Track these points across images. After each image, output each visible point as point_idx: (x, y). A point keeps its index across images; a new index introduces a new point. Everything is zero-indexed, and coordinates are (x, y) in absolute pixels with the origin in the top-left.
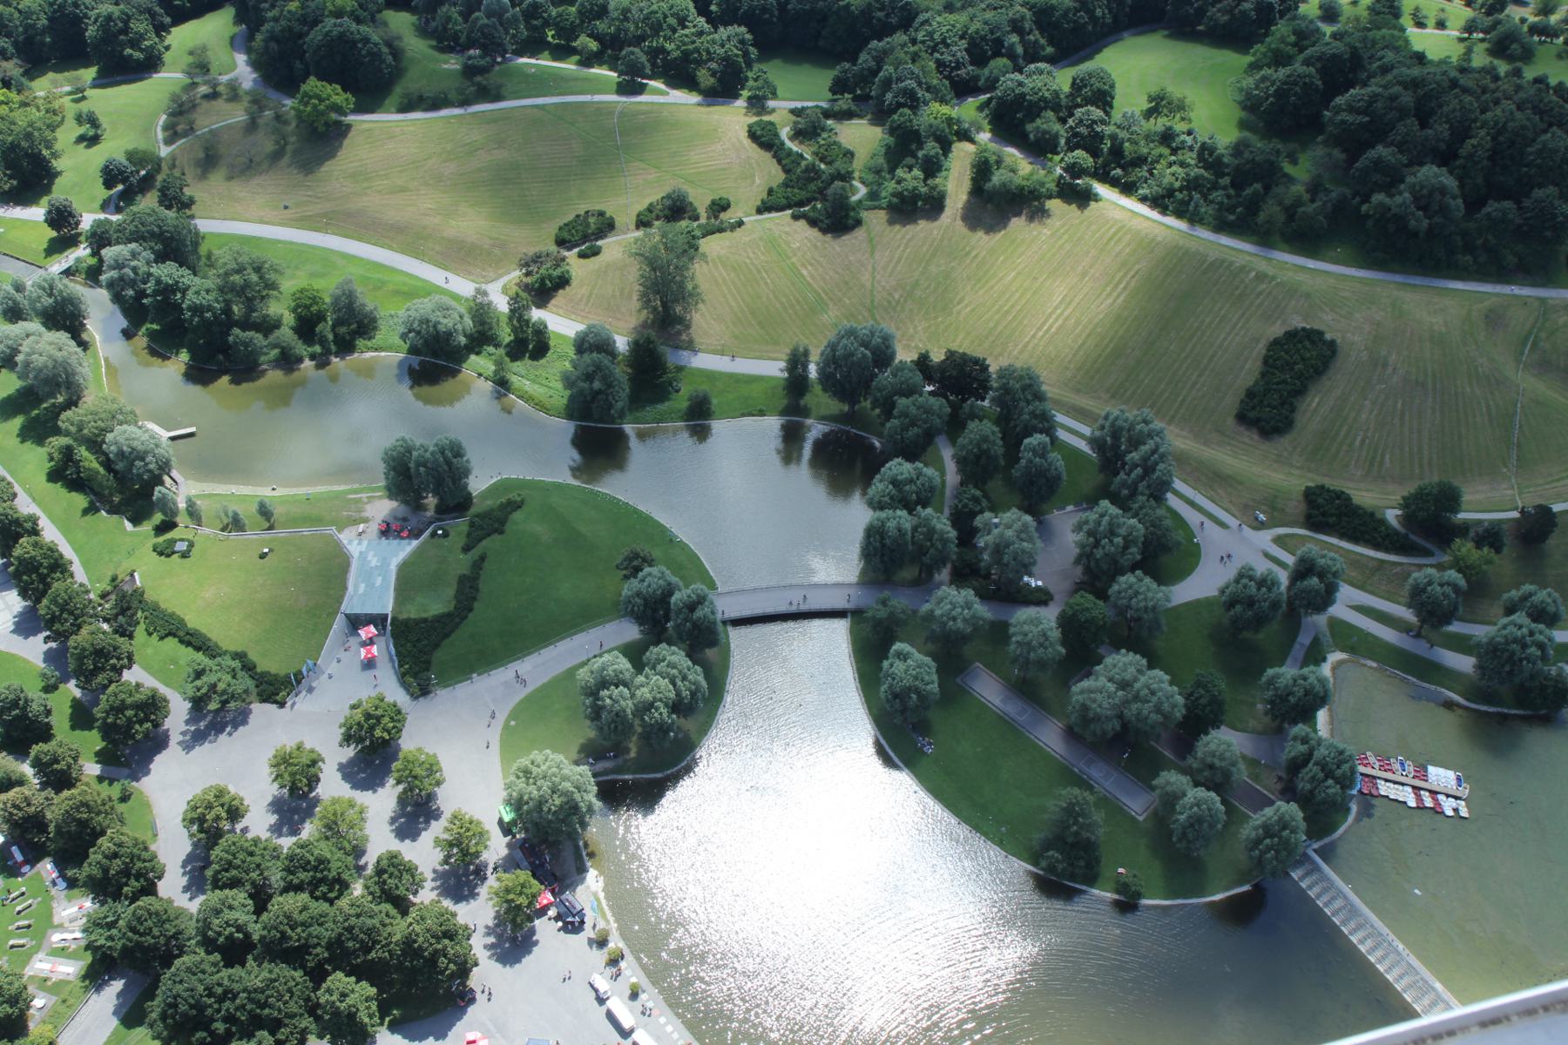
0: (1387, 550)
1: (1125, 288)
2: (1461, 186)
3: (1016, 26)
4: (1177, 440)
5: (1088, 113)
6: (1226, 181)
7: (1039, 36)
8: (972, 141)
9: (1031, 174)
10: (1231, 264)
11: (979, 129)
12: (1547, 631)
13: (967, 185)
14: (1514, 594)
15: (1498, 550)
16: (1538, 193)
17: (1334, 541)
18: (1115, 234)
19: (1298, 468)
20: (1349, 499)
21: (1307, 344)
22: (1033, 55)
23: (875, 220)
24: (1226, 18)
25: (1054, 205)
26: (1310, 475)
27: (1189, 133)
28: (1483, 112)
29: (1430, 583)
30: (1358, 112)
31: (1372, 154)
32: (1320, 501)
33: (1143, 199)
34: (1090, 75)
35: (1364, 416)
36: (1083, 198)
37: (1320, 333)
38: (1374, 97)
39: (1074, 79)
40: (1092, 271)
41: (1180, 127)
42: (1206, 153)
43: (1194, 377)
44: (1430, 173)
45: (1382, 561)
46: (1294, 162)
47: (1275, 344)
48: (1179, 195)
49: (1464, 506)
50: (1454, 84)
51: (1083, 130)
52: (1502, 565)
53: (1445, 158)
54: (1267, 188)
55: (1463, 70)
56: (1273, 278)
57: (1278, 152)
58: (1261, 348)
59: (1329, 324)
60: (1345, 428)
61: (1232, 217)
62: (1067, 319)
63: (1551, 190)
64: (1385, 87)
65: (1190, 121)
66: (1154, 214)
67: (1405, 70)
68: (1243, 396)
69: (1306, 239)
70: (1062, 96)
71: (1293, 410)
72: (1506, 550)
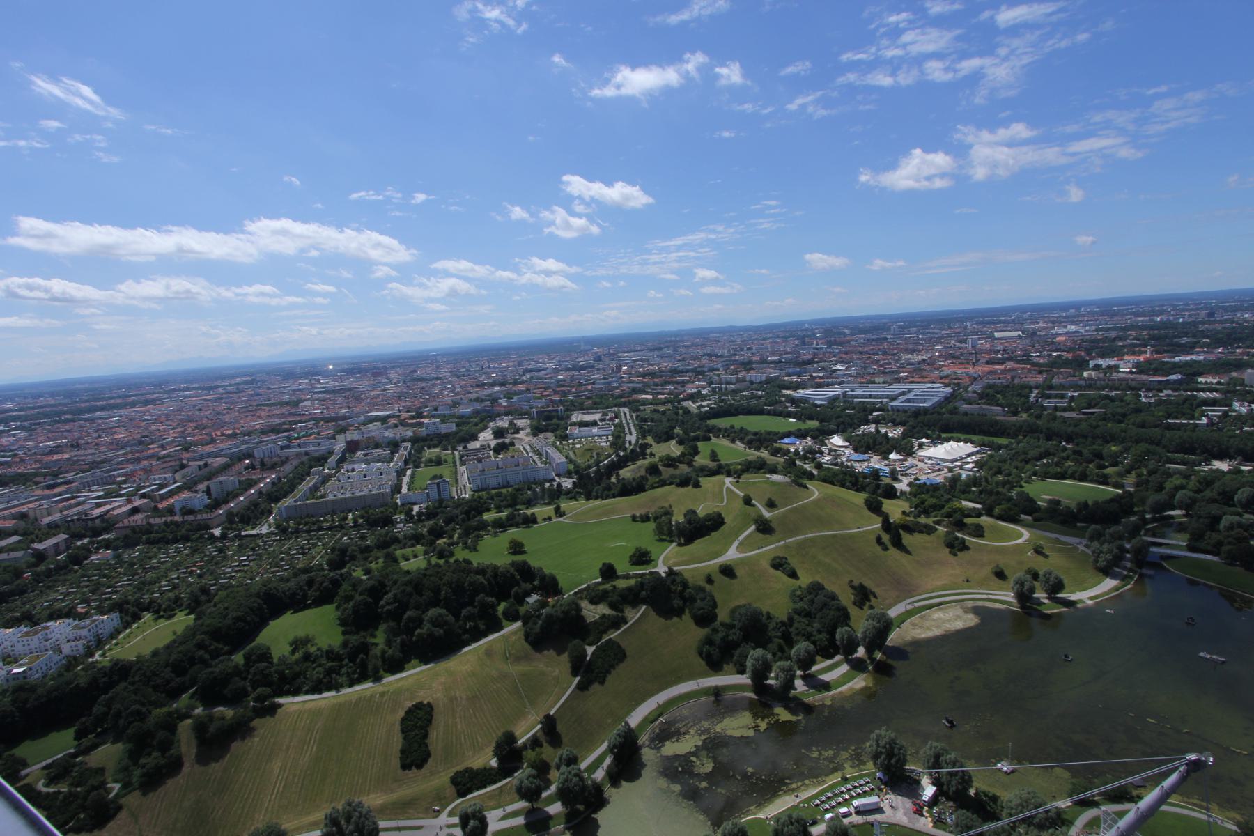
0: (500, 781)
1: (315, 741)
2: (448, 610)
3: (200, 646)
4: (373, 800)
5: (257, 668)
6: (346, 661)
7: (216, 644)
8: (189, 716)
9: (234, 715)
10: (365, 697)
11: (194, 708)
12: (576, 767)
13: (194, 742)
14: (557, 760)
15: (541, 746)
16: (478, 599)
17: (475, 794)
18: (298, 716)
19: (444, 771)
20: (471, 768)
21: (418, 711)
22: (216, 654)
23: (133, 799)
24: (318, 593)
25: (256, 722)
26: (449, 771)
27: (318, 649)
28: (441, 580)
29: (522, 782)
30: (391, 603)
31: (405, 616)
32: (459, 780)
33: (307, 693)
34: (252, 649)
35: (459, 727)
36: (273, 709)
37: (421, 703)
38: (395, 595)
39: (244, 655)
40: (292, 744)
41: (313, 649)
42: (331, 655)
43: (371, 762)
44: (433, 612)
45: (501, 787)
46: (374, 636)
47: (403, 719)
48: (325, 680)
49: (518, 737)
50: (425, 575)
51: (258, 677)
52: (549, 753)
53: (435, 603)
54: (367, 654)
55: (426, 569)
56: (388, 691)
57: (364, 636)
58: (398, 727)
59: (424, 697)
60: (454, 738)
61: (356, 676)
62: (287, 777)
63: (482, 595)
64: (398, 589)
65: (317, 644)
66: (316, 696)
67: (403, 579)
68: (399, 755)
69: (395, 666)
70: (240, 667)
71: (427, 746)
72: (545, 744)
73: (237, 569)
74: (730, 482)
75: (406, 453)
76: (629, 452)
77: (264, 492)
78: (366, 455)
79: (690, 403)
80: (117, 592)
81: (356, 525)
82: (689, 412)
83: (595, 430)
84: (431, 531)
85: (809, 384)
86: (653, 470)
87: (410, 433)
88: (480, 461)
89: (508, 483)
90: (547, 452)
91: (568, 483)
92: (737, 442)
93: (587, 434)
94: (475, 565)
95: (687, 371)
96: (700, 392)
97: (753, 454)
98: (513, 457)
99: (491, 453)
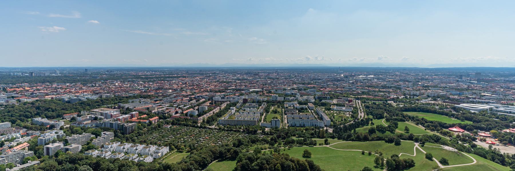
73: (204, 139)
74: (418, 145)
75: (264, 106)
76: (360, 120)
77: (215, 113)
78: (250, 105)
79: (393, 102)
80: (169, 139)
81: (244, 131)
82: (392, 106)
83: (344, 108)
84: (272, 139)
85: (465, 100)
86: (372, 131)
87: (266, 99)
88: (293, 114)
89: (304, 125)
90: (322, 115)
91: (331, 130)
92: (419, 125)
93: (340, 109)
94: (290, 157)
95: (391, 87)
96: (398, 98)
97: (430, 133)
98: (307, 115)
99: (297, 111)
